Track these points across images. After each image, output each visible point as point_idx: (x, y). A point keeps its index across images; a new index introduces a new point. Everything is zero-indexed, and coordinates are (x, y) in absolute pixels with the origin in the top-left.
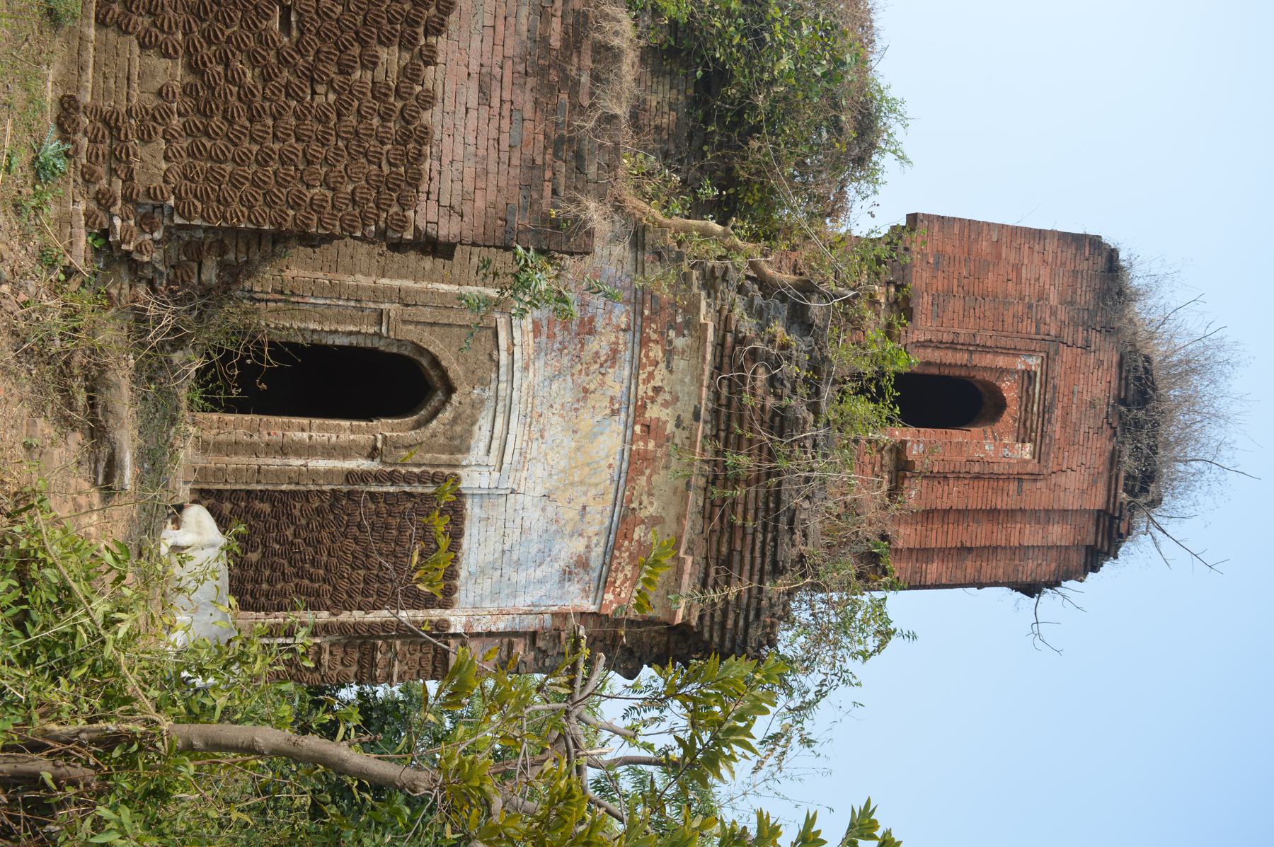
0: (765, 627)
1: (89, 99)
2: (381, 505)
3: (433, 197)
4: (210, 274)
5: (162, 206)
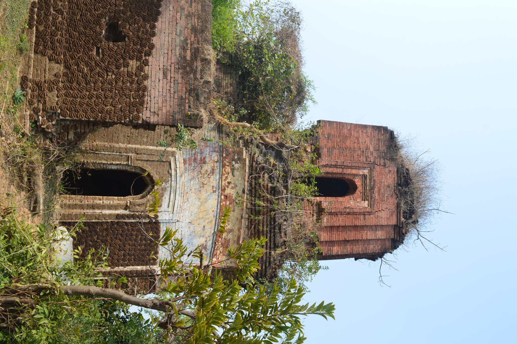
0: (273, 269)
1: (31, 77)
2: (129, 227)
3: (148, 109)
4: (71, 136)
5: (55, 113)
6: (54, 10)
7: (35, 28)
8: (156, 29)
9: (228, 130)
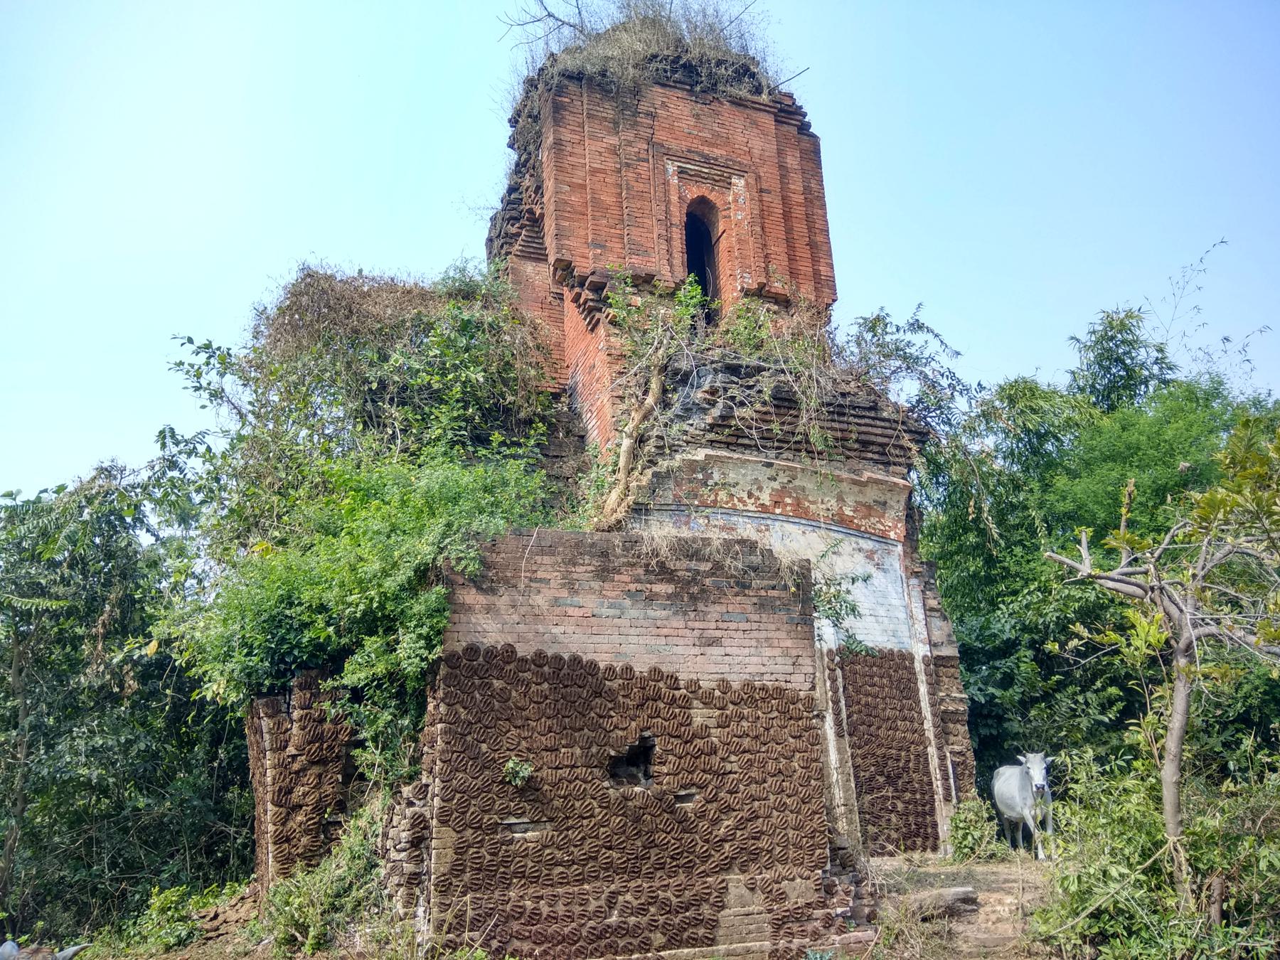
6: (611, 916)
7: (662, 953)
8: (615, 664)
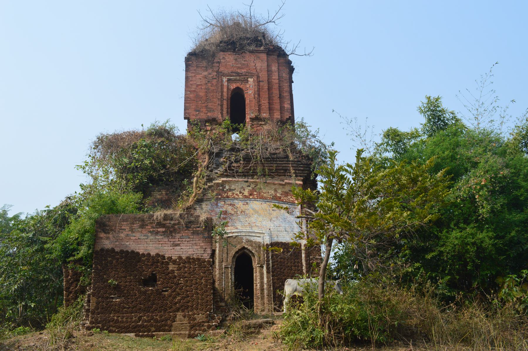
4: (223, 304)
9: (202, 195)
